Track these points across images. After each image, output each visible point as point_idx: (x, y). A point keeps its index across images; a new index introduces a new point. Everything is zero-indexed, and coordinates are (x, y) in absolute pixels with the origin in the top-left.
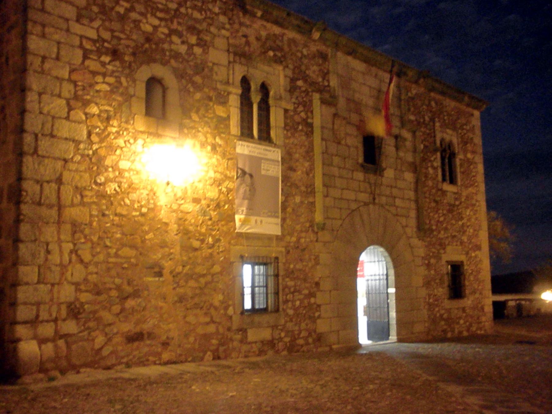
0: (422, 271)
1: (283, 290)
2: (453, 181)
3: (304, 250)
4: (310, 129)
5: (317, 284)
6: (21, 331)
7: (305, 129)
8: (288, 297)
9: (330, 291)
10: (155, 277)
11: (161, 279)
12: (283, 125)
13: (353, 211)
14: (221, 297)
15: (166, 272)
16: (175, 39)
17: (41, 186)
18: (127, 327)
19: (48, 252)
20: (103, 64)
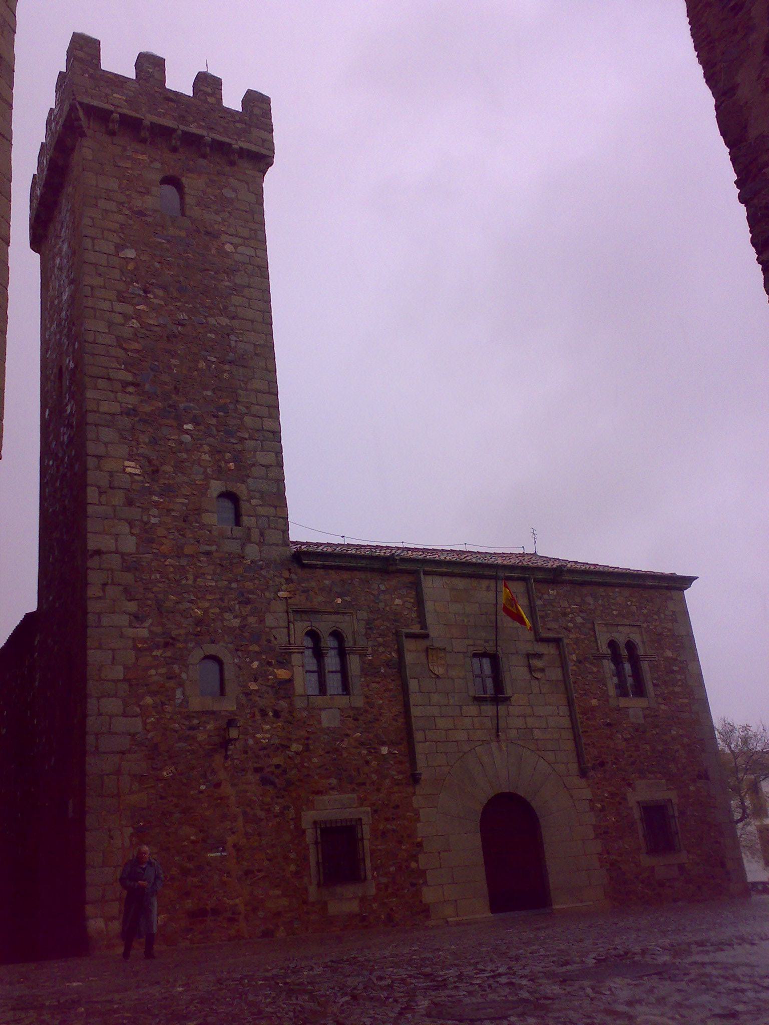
1: (372, 854)
2: (640, 691)
5: (420, 845)
14: (293, 868)
16: (227, 616)
18: (189, 904)
19: (111, 837)
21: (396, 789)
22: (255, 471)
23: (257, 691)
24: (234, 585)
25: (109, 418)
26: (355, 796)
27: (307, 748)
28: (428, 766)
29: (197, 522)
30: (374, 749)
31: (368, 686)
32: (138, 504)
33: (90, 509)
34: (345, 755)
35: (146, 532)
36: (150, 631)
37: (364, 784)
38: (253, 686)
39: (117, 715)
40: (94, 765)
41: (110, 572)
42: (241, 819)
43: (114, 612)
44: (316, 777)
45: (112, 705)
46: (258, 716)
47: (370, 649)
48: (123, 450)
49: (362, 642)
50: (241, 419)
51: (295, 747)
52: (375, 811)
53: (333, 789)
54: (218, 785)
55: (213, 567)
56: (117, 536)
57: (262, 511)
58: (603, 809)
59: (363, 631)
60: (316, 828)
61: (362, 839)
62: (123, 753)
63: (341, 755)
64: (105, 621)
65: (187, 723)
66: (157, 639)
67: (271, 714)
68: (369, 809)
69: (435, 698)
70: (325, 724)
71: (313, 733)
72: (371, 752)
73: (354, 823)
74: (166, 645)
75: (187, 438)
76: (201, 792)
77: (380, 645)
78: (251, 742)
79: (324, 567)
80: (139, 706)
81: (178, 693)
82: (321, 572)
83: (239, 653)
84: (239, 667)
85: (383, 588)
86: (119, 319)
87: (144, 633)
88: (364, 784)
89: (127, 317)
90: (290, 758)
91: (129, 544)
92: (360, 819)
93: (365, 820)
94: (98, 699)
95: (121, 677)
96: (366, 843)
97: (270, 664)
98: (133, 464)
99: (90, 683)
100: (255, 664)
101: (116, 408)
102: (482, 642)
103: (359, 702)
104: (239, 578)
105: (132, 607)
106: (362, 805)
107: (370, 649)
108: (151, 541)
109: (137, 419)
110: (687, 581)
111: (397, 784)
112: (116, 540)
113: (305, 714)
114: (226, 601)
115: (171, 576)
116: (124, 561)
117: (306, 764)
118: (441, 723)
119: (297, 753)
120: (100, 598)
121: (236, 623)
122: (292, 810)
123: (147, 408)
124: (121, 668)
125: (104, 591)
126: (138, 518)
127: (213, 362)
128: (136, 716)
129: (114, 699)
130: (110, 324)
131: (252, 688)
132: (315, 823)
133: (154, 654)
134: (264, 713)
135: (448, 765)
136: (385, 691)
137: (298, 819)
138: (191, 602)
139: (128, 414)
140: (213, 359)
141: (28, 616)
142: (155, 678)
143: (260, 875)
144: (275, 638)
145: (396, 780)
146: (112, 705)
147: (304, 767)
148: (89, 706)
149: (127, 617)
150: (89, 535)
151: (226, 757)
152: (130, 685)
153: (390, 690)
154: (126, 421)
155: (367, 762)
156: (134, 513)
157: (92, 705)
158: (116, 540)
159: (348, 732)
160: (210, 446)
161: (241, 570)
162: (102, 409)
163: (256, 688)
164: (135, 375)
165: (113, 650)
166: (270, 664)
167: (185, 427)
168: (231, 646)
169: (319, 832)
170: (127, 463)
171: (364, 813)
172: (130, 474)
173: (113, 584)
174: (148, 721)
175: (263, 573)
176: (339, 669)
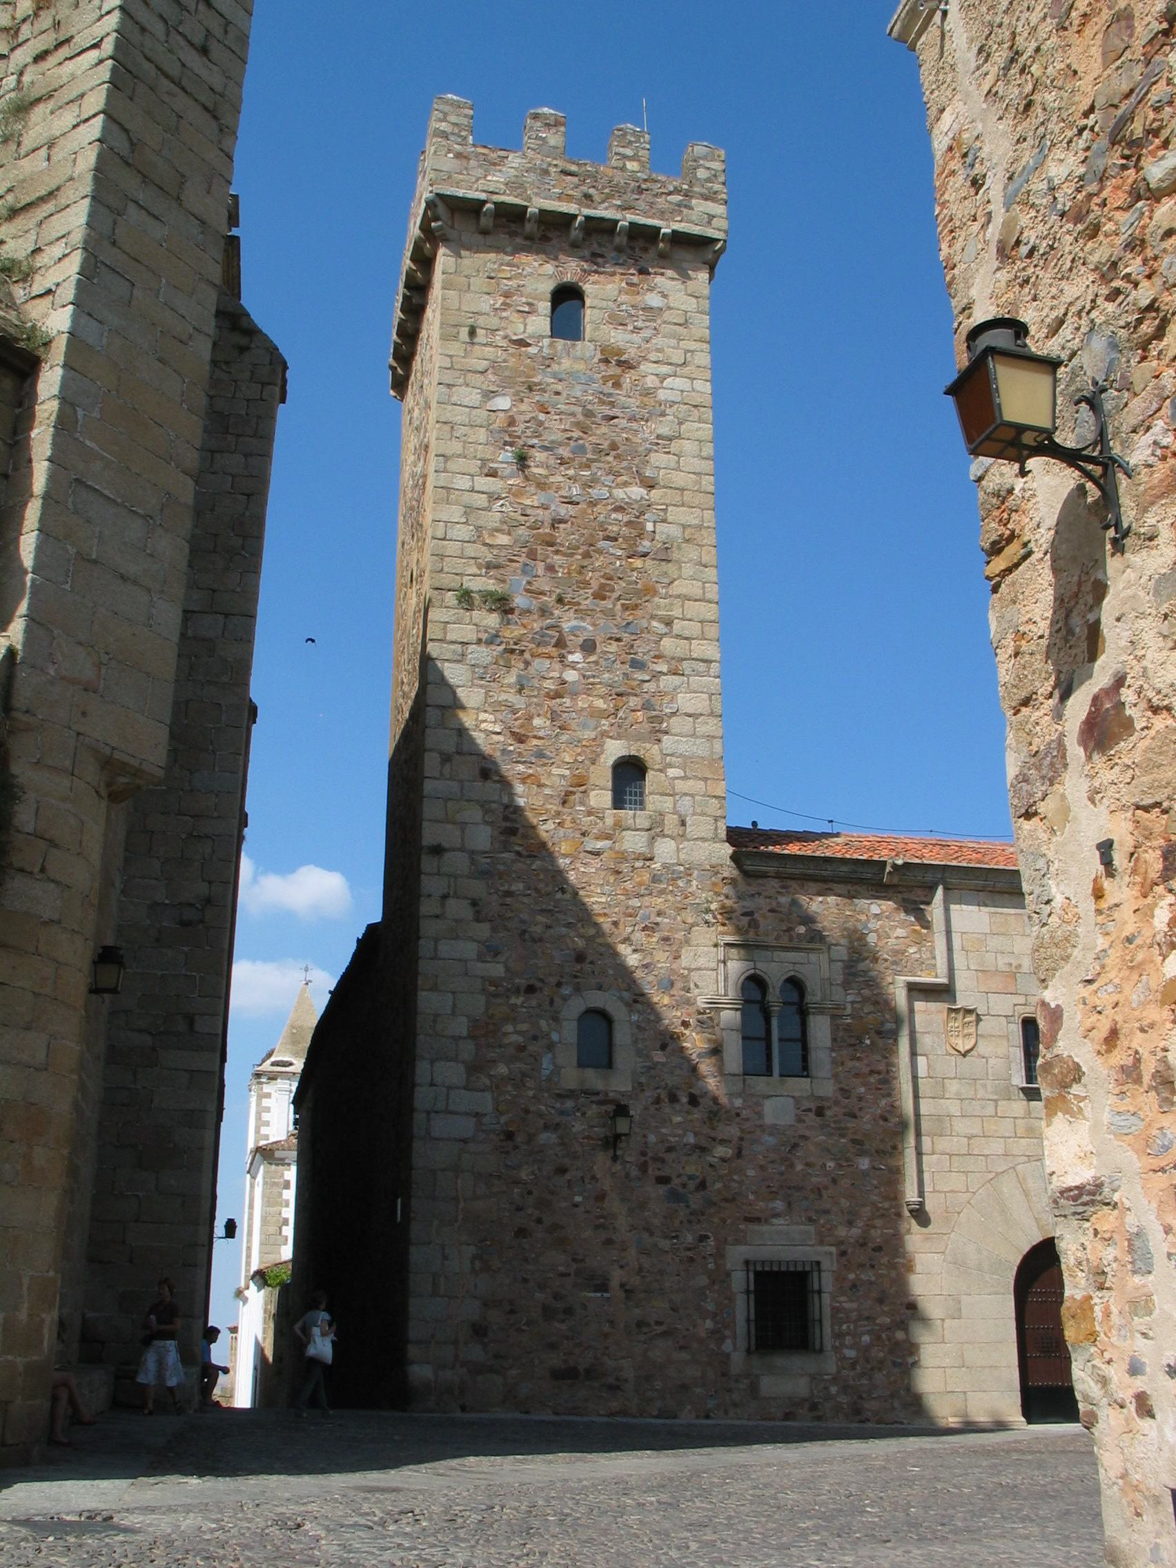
1: (833, 1316)
3: (878, 1249)
8: (844, 1327)
9: (943, 1320)
11: (606, 1295)
12: (829, 1044)
14: (709, 1324)
15: (614, 1283)
18: (555, 1360)
19: (445, 1258)
20: (514, 1008)
21: (878, 1222)
22: (675, 724)
23: (663, 1064)
24: (635, 902)
25: (458, 648)
26: (811, 1228)
27: (739, 1154)
29: (582, 803)
30: (847, 1160)
31: (842, 1064)
33: (428, 786)
34: (799, 1167)
35: (506, 818)
36: (507, 969)
37: (827, 1212)
39: (458, 1088)
40: (424, 1156)
41: (452, 880)
42: (632, 1252)
43: (456, 938)
44: (751, 1197)
45: (452, 1073)
47: (849, 1006)
49: (838, 995)
50: (658, 642)
53: (777, 1215)
54: (601, 1197)
55: (603, 873)
56: (463, 826)
57: (681, 786)
59: (839, 979)
60: (748, 1271)
61: (820, 1292)
62: (465, 1141)
63: (792, 1166)
64: (445, 948)
65: (558, 1105)
66: (517, 981)
67: (684, 1100)
68: (833, 1249)
69: (953, 1087)
70: (769, 1120)
71: (750, 1133)
73: (807, 1268)
74: (531, 989)
75: (571, 676)
76: (576, 1205)
77: (865, 1000)
78: (652, 1138)
79: (778, 876)
81: (546, 1062)
82: (775, 883)
83: (639, 1006)
84: (639, 1027)
86: (482, 500)
87: (498, 970)
88: (827, 1212)
89: (493, 497)
90: (711, 1166)
92: (818, 1263)
93: (826, 1264)
94: (432, 1062)
95: (465, 1033)
96: (826, 1299)
98: (491, 718)
99: (421, 1038)
101: (469, 633)
103: (827, 1089)
105: (483, 930)
106: (821, 1243)
107: (849, 1006)
108: (512, 832)
111: (883, 1215)
112: (463, 831)
114: (621, 926)
115: (541, 886)
116: (473, 861)
118: (960, 1126)
119: (723, 1160)
120: (437, 917)
122: (711, 1242)
124: (464, 1019)
126: (496, 798)
127: (619, 557)
128: (483, 1091)
129: (452, 1064)
130: (469, 510)
131: (656, 1059)
132: (747, 1263)
133: (513, 1001)
134: (673, 1099)
135: (967, 1191)
136: (872, 1072)
137: (719, 1255)
138: (569, 925)
139: (489, 642)
140: (619, 553)
143: (660, 1329)
144: (696, 985)
145: (878, 1209)
146: (452, 1073)
148: (418, 1071)
149: (474, 945)
150: (425, 824)
151: (615, 1158)
153: (879, 1073)
154: (482, 655)
155: (834, 1181)
157: (422, 1070)
158: (463, 831)
159: (807, 1133)
161: (646, 877)
162: (450, 637)
163: (663, 1060)
165: (453, 993)
167: (571, 658)
168: (626, 995)
169: (752, 1276)
170: (483, 716)
171: (826, 1255)
174: (502, 1098)
175: (680, 883)
176: (798, 1036)
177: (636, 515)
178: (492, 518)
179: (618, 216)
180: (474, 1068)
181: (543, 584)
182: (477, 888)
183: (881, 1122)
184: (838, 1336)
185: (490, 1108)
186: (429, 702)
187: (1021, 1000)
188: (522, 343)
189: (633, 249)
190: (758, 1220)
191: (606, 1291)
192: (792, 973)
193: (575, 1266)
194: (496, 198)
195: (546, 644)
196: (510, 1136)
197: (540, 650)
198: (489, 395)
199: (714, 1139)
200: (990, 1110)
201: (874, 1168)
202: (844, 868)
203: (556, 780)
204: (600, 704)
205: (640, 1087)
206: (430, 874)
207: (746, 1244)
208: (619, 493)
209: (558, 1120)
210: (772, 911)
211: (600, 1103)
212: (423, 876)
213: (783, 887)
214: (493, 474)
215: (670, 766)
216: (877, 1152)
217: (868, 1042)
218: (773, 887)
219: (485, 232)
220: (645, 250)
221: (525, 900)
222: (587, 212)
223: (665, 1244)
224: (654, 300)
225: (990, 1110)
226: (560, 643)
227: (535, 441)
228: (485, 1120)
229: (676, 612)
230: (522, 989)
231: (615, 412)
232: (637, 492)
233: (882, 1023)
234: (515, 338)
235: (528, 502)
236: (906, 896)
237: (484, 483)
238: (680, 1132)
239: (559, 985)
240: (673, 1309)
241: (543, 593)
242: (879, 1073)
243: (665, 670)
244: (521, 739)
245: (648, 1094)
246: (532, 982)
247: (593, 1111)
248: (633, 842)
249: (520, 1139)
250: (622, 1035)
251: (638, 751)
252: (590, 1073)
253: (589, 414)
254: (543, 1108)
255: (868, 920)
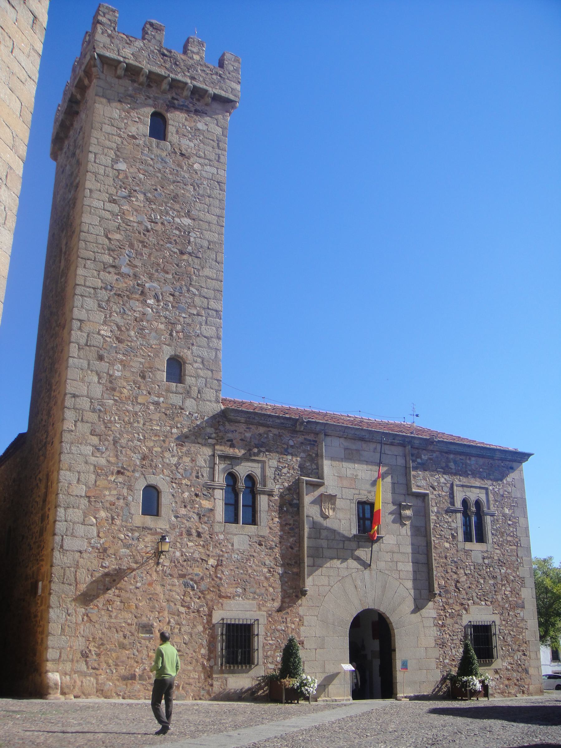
0: (434, 632)
1: (264, 647)
2: (481, 539)
4: (296, 509)
6: (49, 665)
7: (291, 510)
8: (269, 653)
9: (316, 649)
10: (148, 633)
11: (151, 635)
13: (343, 577)
16: (167, 455)
17: (64, 570)
28: (314, 585)
30: (273, 568)
32: (106, 360)
33: (71, 360)
36: (108, 461)
38: (183, 511)
44: (226, 586)
45: (76, 515)
46: (185, 535)
48: (100, 317)
51: (212, 562)
52: (270, 615)
53: (239, 596)
55: (159, 415)
57: (201, 373)
58: (443, 625)
61: (258, 635)
67: (195, 534)
72: (270, 571)
76: (137, 588)
80: (95, 518)
84: (173, 495)
85: (291, 443)
91: (97, 391)
92: (258, 620)
94: (66, 509)
95: (83, 494)
96: (261, 638)
97: (197, 495)
100: (186, 495)
102: (366, 493)
104: (179, 425)
105: (95, 440)
106: (260, 609)
108: (114, 389)
109: (112, 293)
110: (524, 457)
111: (289, 597)
113: (221, 537)
114: (167, 443)
117: (218, 575)
121: (174, 460)
123: (122, 285)
125: (75, 425)
133: (109, 478)
134: (189, 534)
139: (106, 289)
141: (21, 437)
142: (108, 498)
147: (217, 577)
149: (91, 448)
152: (89, 502)
153: (290, 525)
154: (104, 295)
156: (103, 366)
160: (166, 318)
164: (115, 258)
165: (79, 472)
166: (197, 495)
170: (102, 327)
172: (103, 336)
173: (82, 421)
176: (251, 504)
177: (186, 232)
178: (113, 225)
179: (189, 81)
180: (85, 515)
181: (138, 263)
182: (93, 417)
183: (290, 550)
184: (267, 657)
185: (95, 535)
186: (74, 317)
187: (357, 492)
188: (134, 137)
189: (192, 99)
190: (230, 597)
191: (152, 633)
192: (250, 472)
193: (136, 620)
194: (127, 61)
195: (136, 293)
196: (105, 550)
197: (134, 296)
198: (115, 161)
199: (209, 556)
200: (341, 545)
201: (286, 572)
202: (278, 421)
203: (138, 365)
204: (162, 327)
205: (173, 527)
206: (69, 408)
207: (223, 610)
208: (177, 220)
209: (130, 542)
210: (242, 440)
211: (152, 534)
212: (65, 410)
213: (247, 428)
214: (114, 201)
215: (196, 362)
216: (288, 564)
217: (285, 509)
218: (243, 428)
219: (119, 77)
220: (198, 100)
221: (118, 426)
222: (172, 75)
223: (182, 610)
224: (200, 126)
225: (341, 545)
226: (142, 293)
227: (137, 188)
228: (92, 541)
229: (203, 285)
230: (115, 472)
231: (179, 179)
232: (187, 221)
233: (292, 500)
234: (130, 134)
235: (132, 219)
236: (306, 437)
237: (109, 206)
238: (192, 551)
239: (133, 471)
240: (185, 644)
241: (136, 266)
242: (290, 525)
243: (195, 313)
244: (120, 341)
245: (177, 530)
246: (120, 469)
247: (149, 538)
248: (176, 400)
249: (110, 551)
250: (166, 500)
251: (180, 353)
252: (148, 518)
253: (164, 178)
254: (123, 536)
255: (288, 448)
